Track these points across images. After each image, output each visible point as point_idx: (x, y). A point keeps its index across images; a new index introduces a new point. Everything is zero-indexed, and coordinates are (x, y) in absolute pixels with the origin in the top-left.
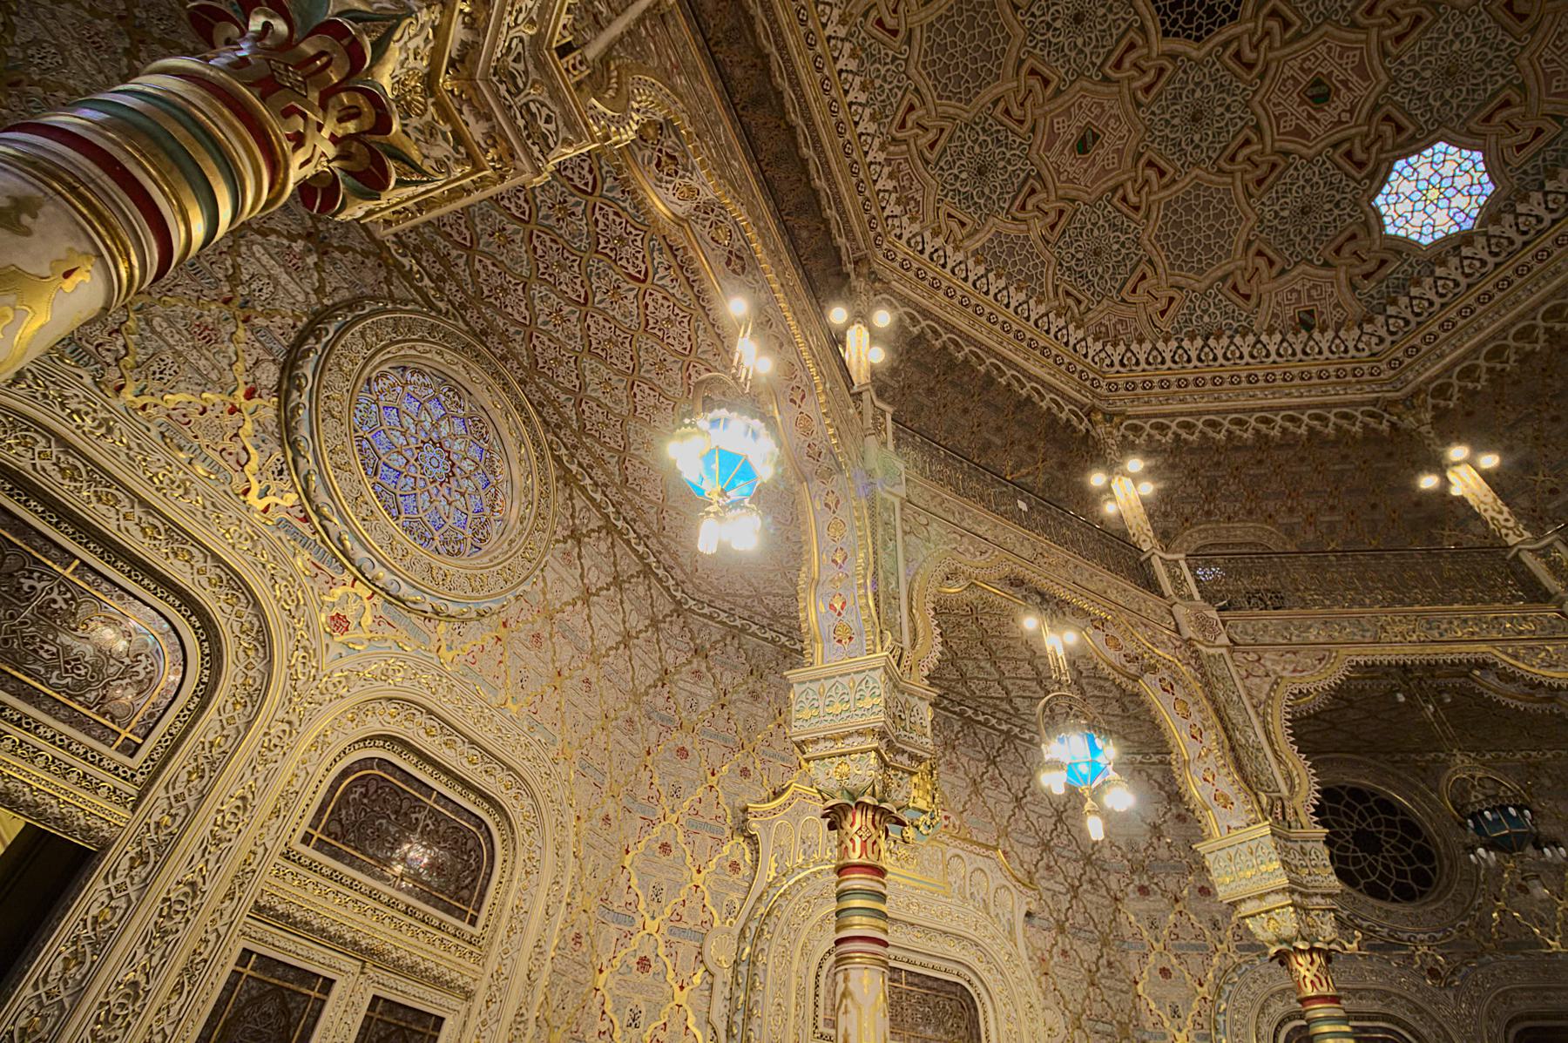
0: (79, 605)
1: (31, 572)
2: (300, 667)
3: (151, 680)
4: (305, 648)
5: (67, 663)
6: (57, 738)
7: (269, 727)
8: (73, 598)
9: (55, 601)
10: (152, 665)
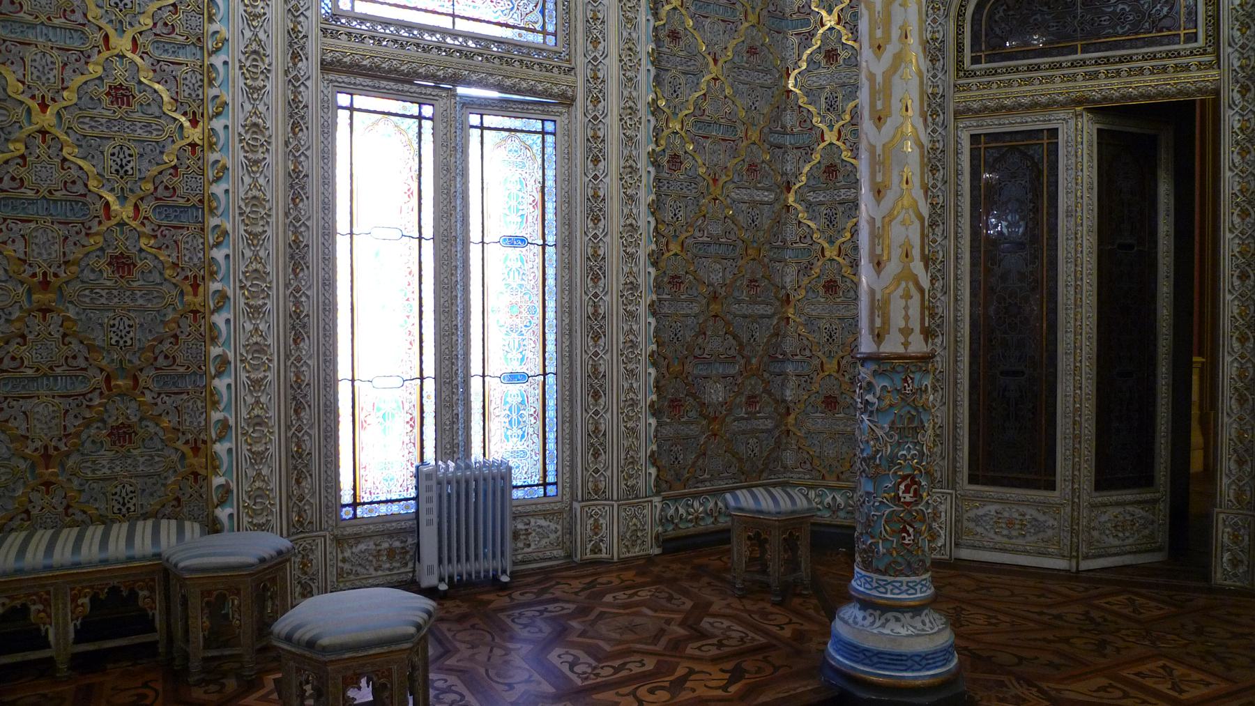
5: (1120, 19)
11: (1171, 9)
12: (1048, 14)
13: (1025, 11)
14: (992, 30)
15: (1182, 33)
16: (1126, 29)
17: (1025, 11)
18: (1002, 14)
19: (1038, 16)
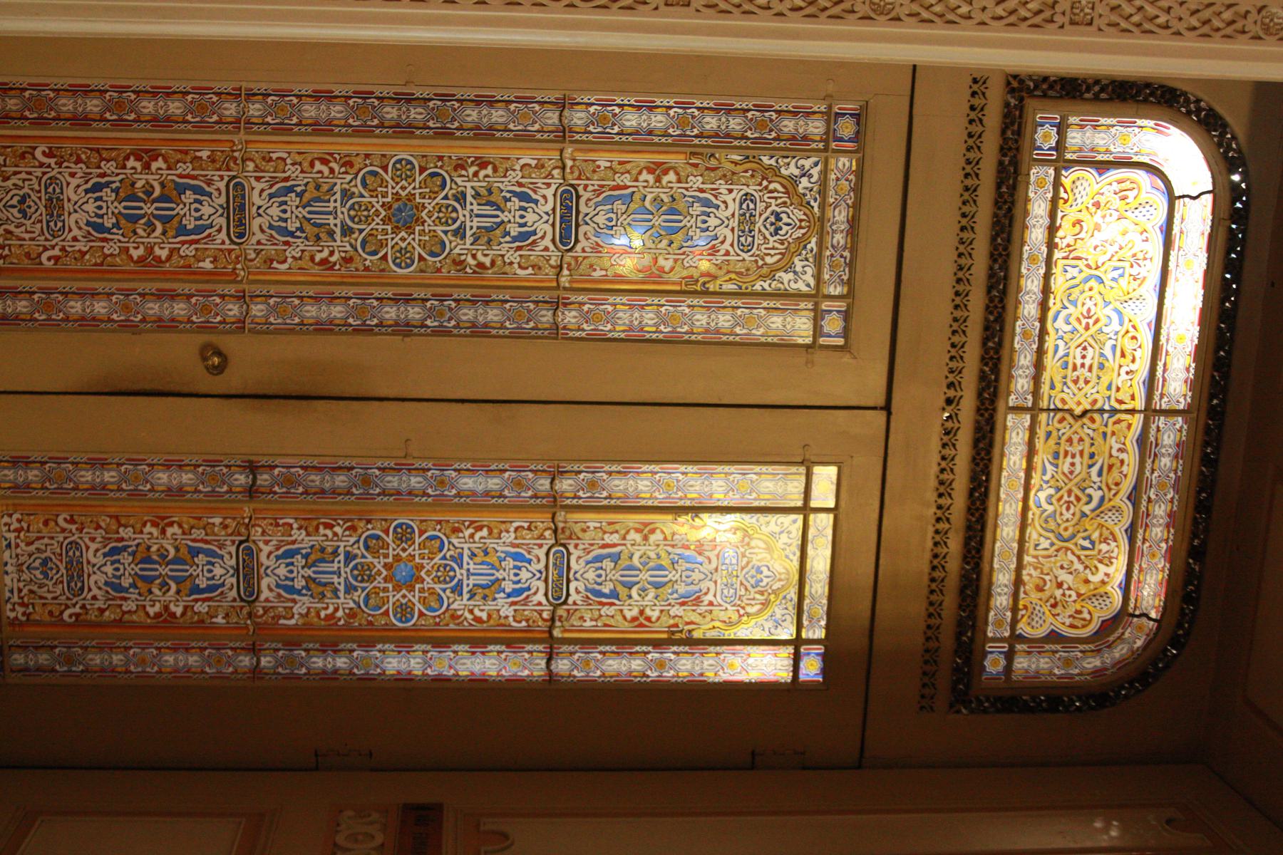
5: (1070, 492)
16: (1045, 505)
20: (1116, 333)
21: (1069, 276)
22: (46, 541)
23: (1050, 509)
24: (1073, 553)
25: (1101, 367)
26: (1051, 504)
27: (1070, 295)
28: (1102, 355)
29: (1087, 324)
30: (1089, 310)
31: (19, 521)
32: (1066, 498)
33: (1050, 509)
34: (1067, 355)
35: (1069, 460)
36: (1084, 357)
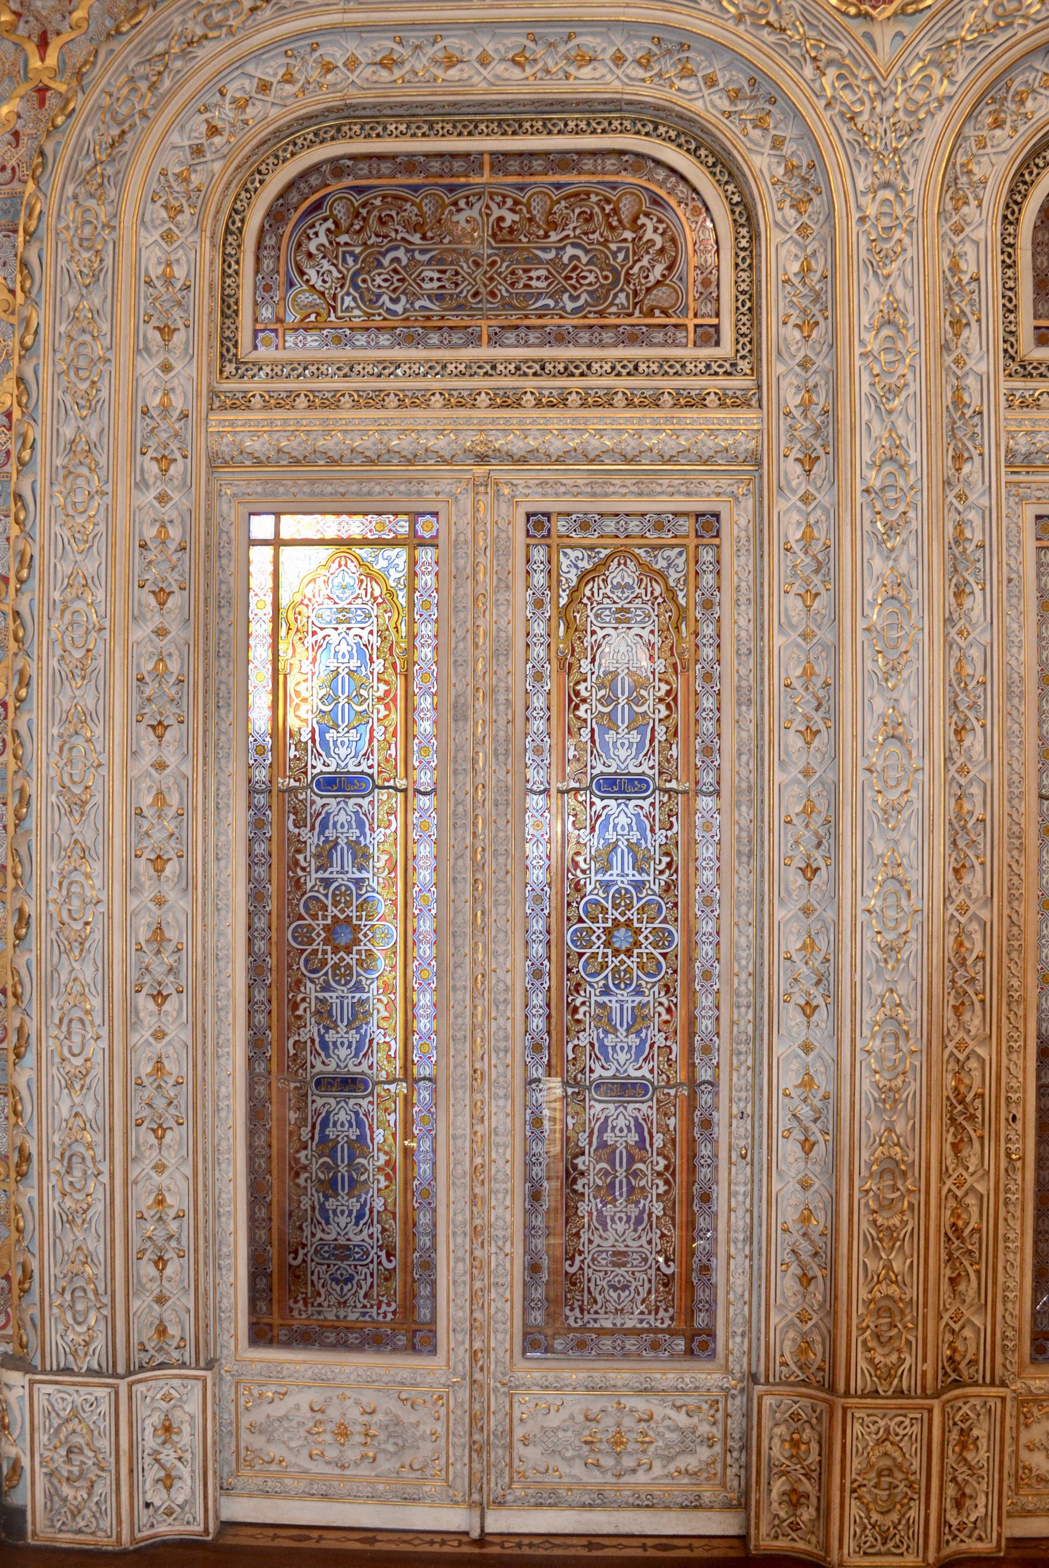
0: (528, 205)
1: (455, 203)
2: (847, 96)
3: (673, 240)
4: (830, 62)
5: (568, 278)
6: (618, 367)
7: (859, 207)
8: (516, 202)
9: (501, 219)
10: (660, 221)
11: (670, 268)
12: (423, 252)
13: (374, 239)
14: (302, 273)
15: (691, 323)
16: (581, 302)
17: (374, 239)
18: (323, 239)
19: (400, 253)
20: (407, 251)
21: (353, 304)
22: (592, 1285)
23: (584, 297)
24: (631, 268)
25: (441, 261)
26: (578, 297)
27: (370, 300)
28: (429, 262)
29: (399, 280)
30: (385, 280)
31: (572, 1309)
32: (573, 282)
33: (584, 297)
34: (429, 297)
35: (534, 283)
36: (431, 280)
